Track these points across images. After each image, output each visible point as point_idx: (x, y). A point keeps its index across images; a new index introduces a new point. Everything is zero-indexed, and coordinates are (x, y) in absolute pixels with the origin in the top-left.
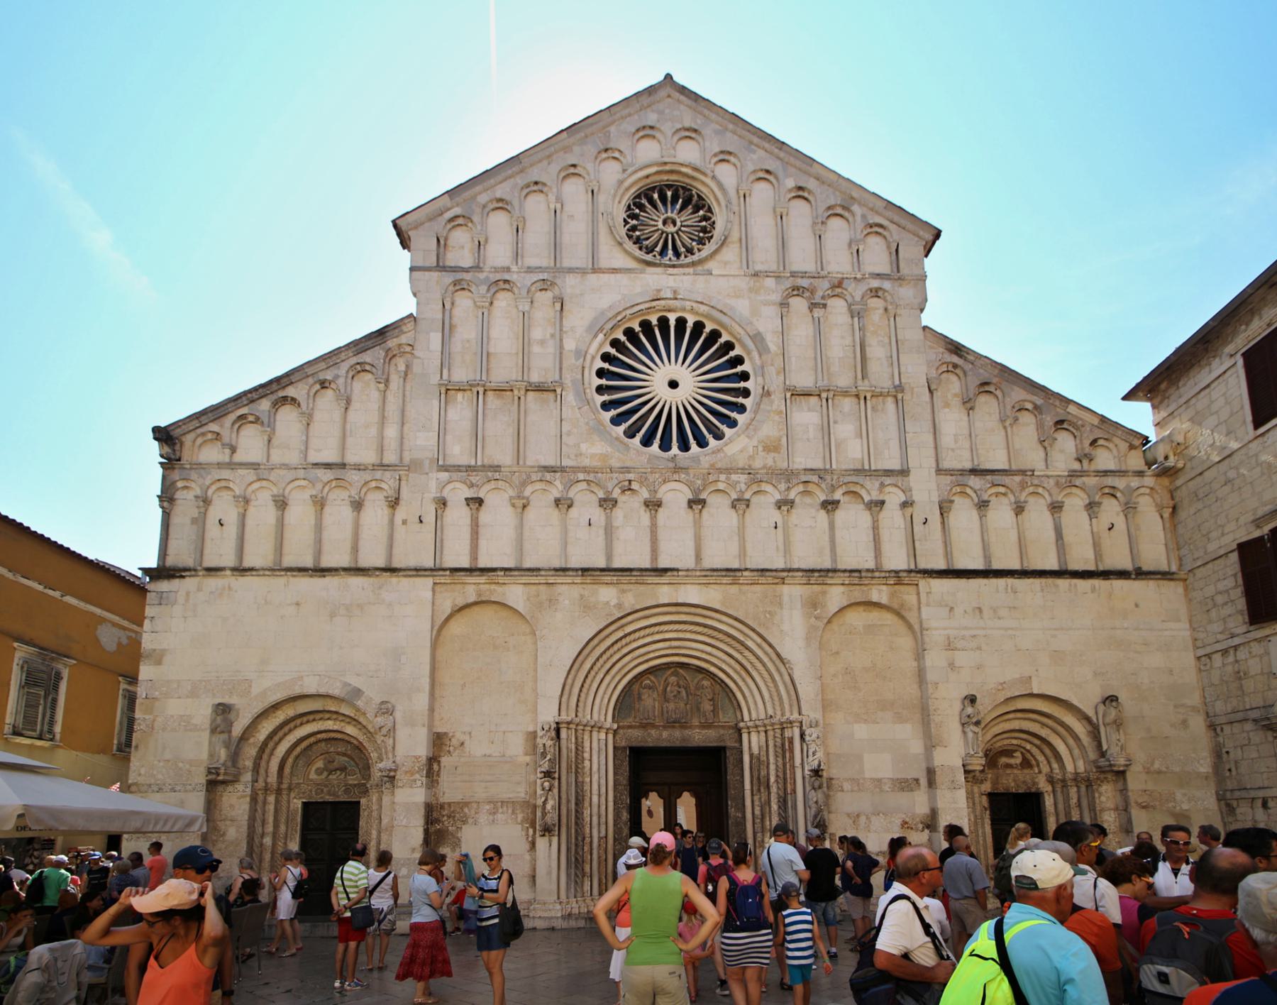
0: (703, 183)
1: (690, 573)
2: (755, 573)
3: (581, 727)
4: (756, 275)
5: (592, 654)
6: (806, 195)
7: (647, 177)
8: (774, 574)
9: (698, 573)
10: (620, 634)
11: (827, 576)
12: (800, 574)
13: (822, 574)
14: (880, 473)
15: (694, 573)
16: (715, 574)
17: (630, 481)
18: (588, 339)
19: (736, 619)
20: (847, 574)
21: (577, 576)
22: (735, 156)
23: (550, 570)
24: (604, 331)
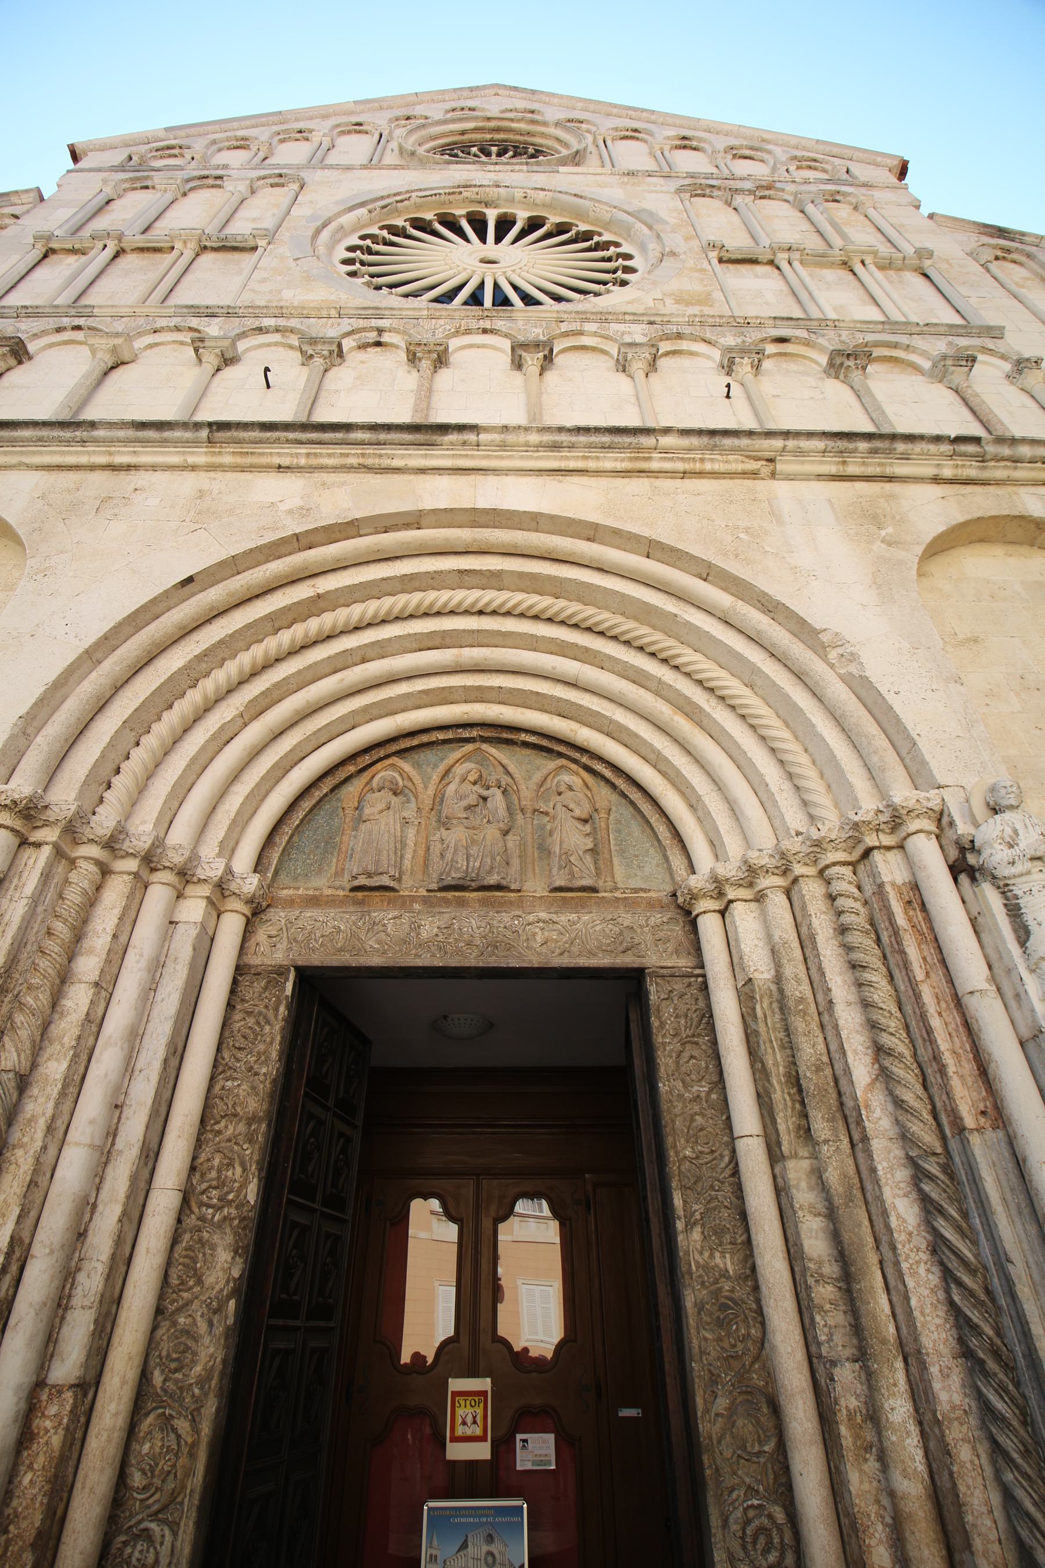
0: (543, 135)
1: (511, 438)
2: (695, 441)
3: (94, 851)
4: (631, 174)
5: (196, 636)
6: (694, 143)
7: (463, 133)
8: (745, 442)
9: (534, 438)
10: (302, 592)
11: (891, 451)
12: (819, 444)
13: (878, 444)
14: (942, 329)
15: (522, 438)
16: (583, 439)
17: (380, 331)
18: (336, 209)
19: (652, 549)
20: (946, 448)
21: (196, 443)
22: (588, 122)
23: (123, 425)
24: (370, 207)
